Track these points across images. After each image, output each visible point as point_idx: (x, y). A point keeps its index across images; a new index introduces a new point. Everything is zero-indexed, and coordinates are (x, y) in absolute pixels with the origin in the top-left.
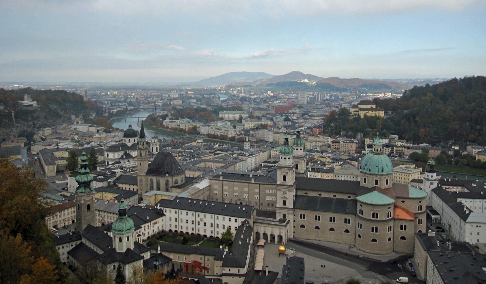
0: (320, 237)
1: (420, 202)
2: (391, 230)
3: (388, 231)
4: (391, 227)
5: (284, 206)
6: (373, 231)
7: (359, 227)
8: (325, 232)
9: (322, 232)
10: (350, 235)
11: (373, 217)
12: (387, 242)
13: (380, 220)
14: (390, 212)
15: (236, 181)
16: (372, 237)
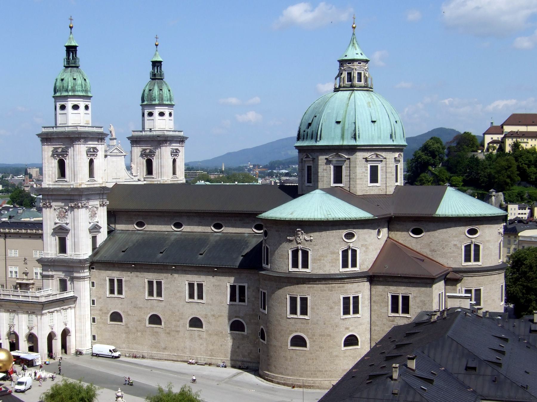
0: (165, 349)
1: (473, 232)
2: (356, 311)
3: (346, 311)
4: (356, 299)
5: (62, 256)
6: (293, 311)
7: (261, 308)
8: (178, 332)
9: (169, 333)
10: (247, 337)
11: (295, 265)
12: (343, 348)
13: (315, 272)
14: (354, 252)
15: (12, 231)
16: (292, 332)
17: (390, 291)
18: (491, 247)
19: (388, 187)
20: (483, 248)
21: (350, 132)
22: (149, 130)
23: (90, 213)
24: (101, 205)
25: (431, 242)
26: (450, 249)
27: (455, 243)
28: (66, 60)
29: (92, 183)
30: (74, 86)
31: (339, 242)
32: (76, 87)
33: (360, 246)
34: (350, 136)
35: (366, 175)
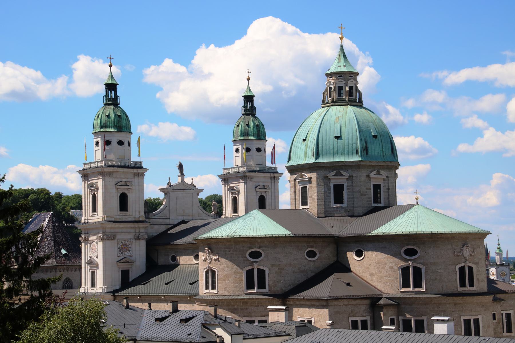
13: (220, 293)
17: (299, 315)
18: (439, 271)
19: (356, 207)
20: (426, 271)
21: (310, 150)
22: (236, 166)
23: (119, 246)
24: (136, 239)
25: (370, 265)
26: (387, 272)
27: (391, 265)
28: (105, 97)
29: (124, 217)
30: (106, 122)
31: (243, 261)
32: (108, 123)
33: (269, 266)
34: (310, 155)
35: (328, 194)
